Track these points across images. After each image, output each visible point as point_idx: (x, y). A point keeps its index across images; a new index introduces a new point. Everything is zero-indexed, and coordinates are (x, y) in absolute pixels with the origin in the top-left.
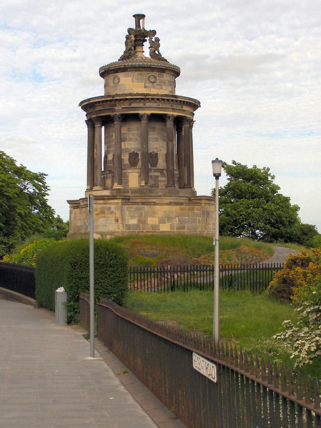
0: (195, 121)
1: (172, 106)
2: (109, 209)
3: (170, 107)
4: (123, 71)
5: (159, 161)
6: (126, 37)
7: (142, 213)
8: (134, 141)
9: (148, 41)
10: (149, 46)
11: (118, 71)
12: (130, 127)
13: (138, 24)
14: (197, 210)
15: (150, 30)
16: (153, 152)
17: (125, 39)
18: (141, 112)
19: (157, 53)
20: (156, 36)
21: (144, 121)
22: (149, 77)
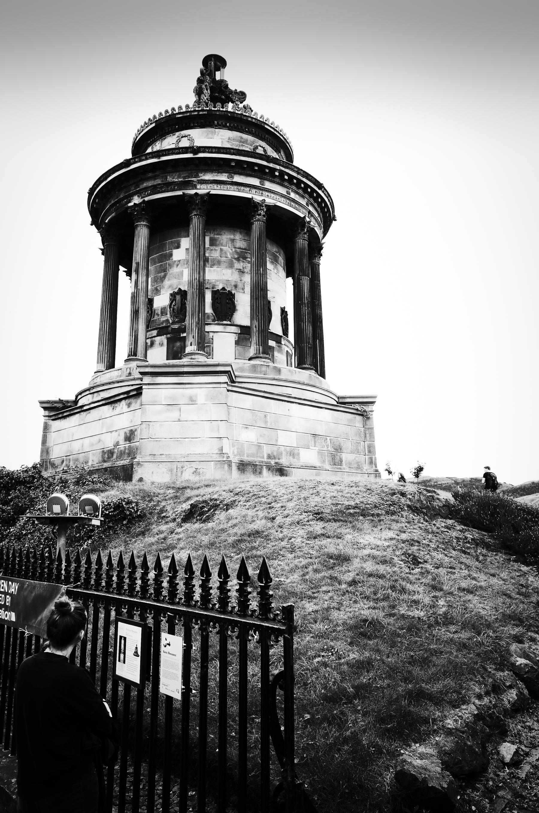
4: (202, 126)
17: (195, 84)
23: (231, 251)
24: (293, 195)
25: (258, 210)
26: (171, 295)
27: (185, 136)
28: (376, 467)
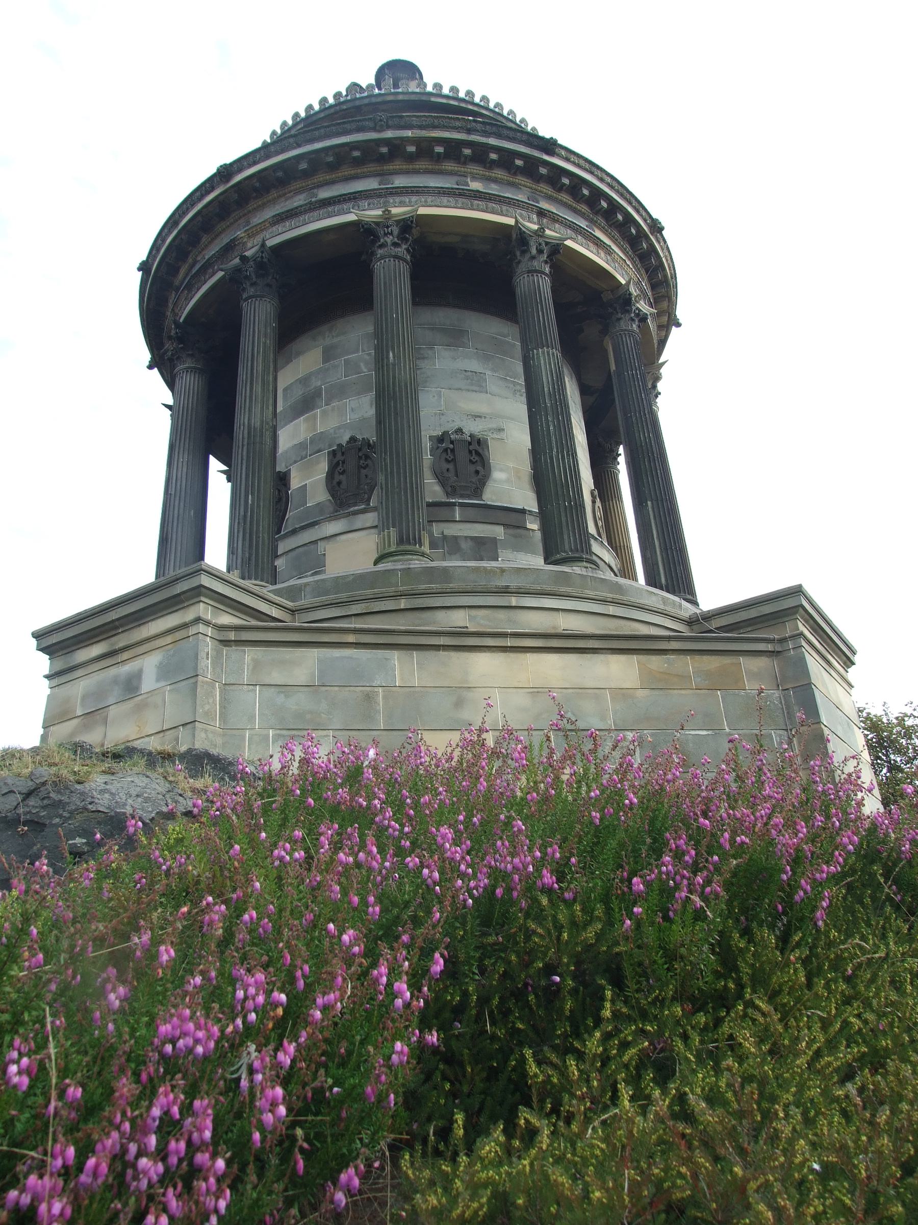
2: (131, 686)
7: (369, 698)
8: (359, 394)
12: (335, 340)
16: (459, 431)
23: (367, 357)
24: (475, 185)
25: (377, 238)
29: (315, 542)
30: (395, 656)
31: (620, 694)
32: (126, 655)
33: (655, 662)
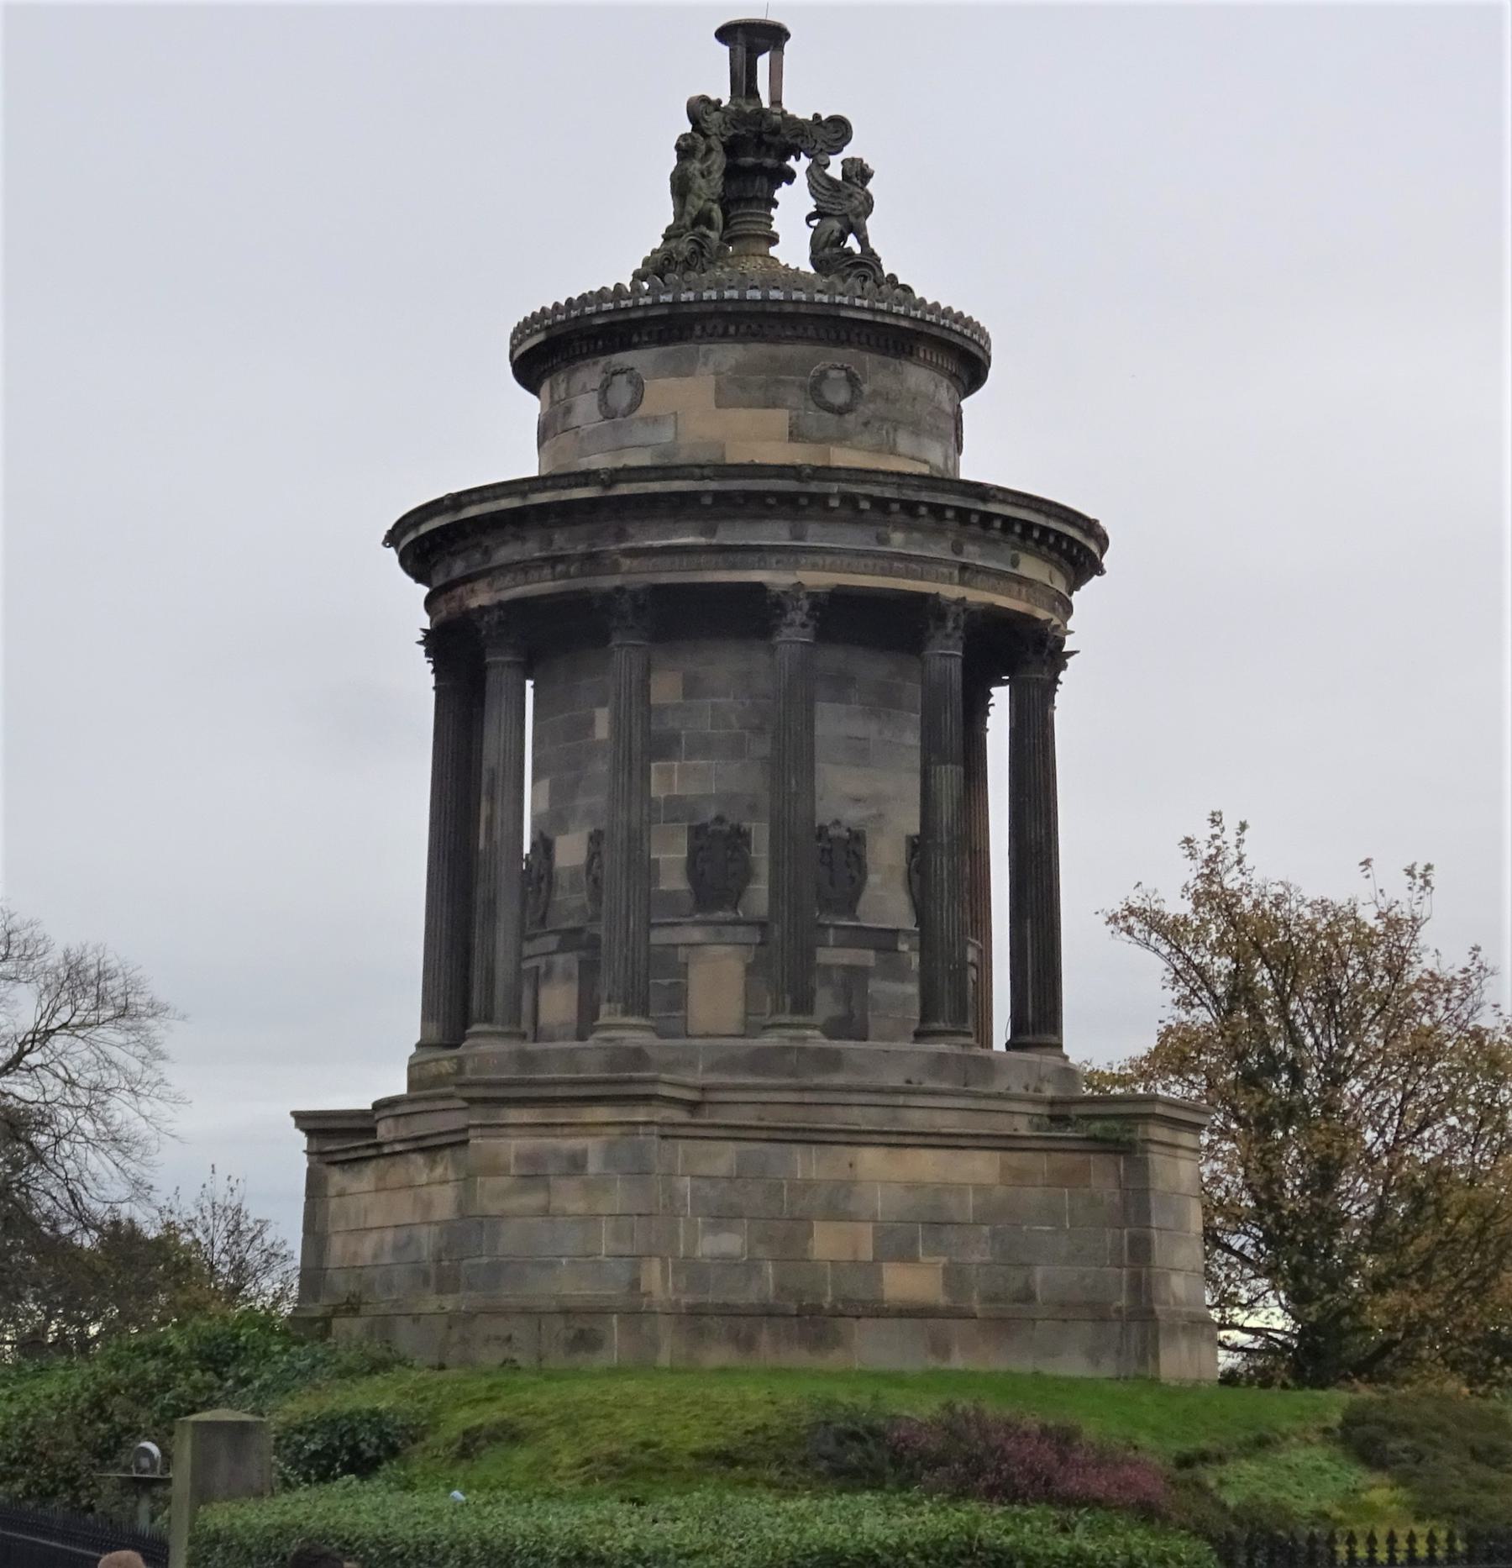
0: (1072, 653)
1: (957, 549)
2: (576, 1164)
3: (950, 556)
4: (661, 340)
5: (873, 878)
6: (678, 147)
9: (801, 180)
10: (810, 205)
11: (635, 339)
13: (743, 81)
14: (1103, 1177)
15: (817, 116)
17: (672, 161)
18: (774, 578)
19: (857, 250)
20: (848, 152)
21: (794, 634)
22: (823, 375)
26: (591, 838)
27: (622, 372)
28: (1150, 1300)
29: (675, 946)
30: (797, 1149)
31: (980, 1188)
32: (567, 1130)
33: (1015, 1159)
